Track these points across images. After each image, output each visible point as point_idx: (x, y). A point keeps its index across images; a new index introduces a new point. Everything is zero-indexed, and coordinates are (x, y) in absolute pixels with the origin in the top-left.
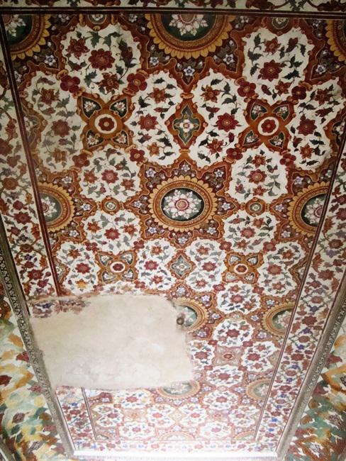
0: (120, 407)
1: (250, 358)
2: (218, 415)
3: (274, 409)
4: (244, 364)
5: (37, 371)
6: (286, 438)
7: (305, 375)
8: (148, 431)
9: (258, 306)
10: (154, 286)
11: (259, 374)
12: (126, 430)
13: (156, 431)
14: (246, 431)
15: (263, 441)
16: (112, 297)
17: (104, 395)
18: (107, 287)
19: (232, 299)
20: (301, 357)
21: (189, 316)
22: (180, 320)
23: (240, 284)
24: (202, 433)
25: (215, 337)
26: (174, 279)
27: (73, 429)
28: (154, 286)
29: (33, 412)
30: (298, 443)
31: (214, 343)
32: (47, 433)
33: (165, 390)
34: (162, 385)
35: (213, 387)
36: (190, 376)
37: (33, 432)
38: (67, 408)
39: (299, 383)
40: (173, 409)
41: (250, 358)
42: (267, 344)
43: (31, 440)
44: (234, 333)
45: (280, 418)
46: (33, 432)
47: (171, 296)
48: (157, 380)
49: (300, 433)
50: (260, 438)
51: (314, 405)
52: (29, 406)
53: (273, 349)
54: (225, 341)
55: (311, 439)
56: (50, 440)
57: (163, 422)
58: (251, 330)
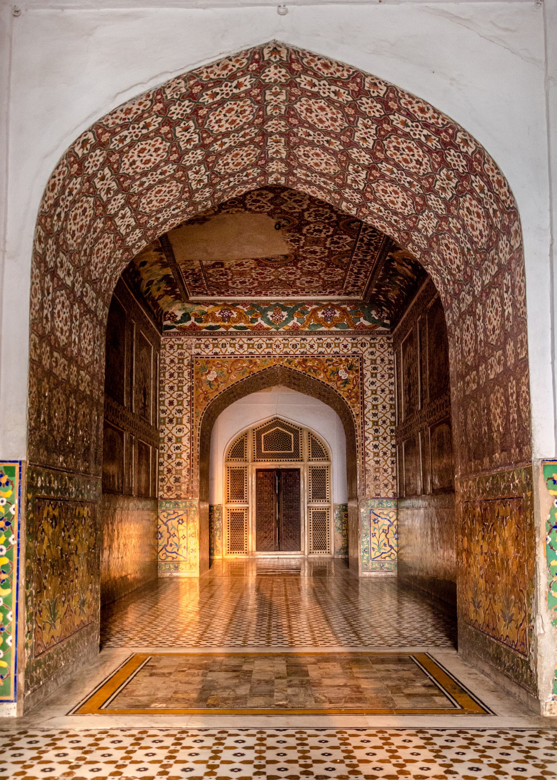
0: (229, 269)
1: (332, 243)
2: (310, 273)
3: (356, 271)
4: (328, 246)
5: (167, 256)
6: (368, 289)
7: (377, 254)
8: (252, 283)
9: (335, 218)
10: (258, 210)
11: (340, 253)
12: (234, 283)
13: (260, 283)
14: (333, 284)
15: (350, 289)
16: (227, 216)
17: (217, 263)
18: (223, 211)
19: (316, 215)
20: (372, 245)
21: (283, 222)
22: (278, 227)
23: (321, 209)
24: (298, 284)
25: (304, 231)
26: (272, 207)
27: (189, 284)
28: (258, 210)
29: (159, 277)
30: (379, 292)
31: (305, 235)
32: (169, 289)
33: (267, 259)
34: (264, 256)
35: (305, 258)
36: (286, 252)
37: (159, 289)
38: (186, 272)
39: (373, 257)
40: (273, 270)
41: (332, 243)
42: (344, 237)
43: (156, 294)
44: (320, 231)
45: (362, 276)
46: (159, 289)
47: (271, 214)
48: (261, 253)
49: (378, 286)
50: (347, 287)
51: (386, 271)
52: (159, 275)
53: (349, 239)
54: (312, 234)
55: (388, 291)
56: (172, 292)
57: (266, 278)
58: (332, 230)
